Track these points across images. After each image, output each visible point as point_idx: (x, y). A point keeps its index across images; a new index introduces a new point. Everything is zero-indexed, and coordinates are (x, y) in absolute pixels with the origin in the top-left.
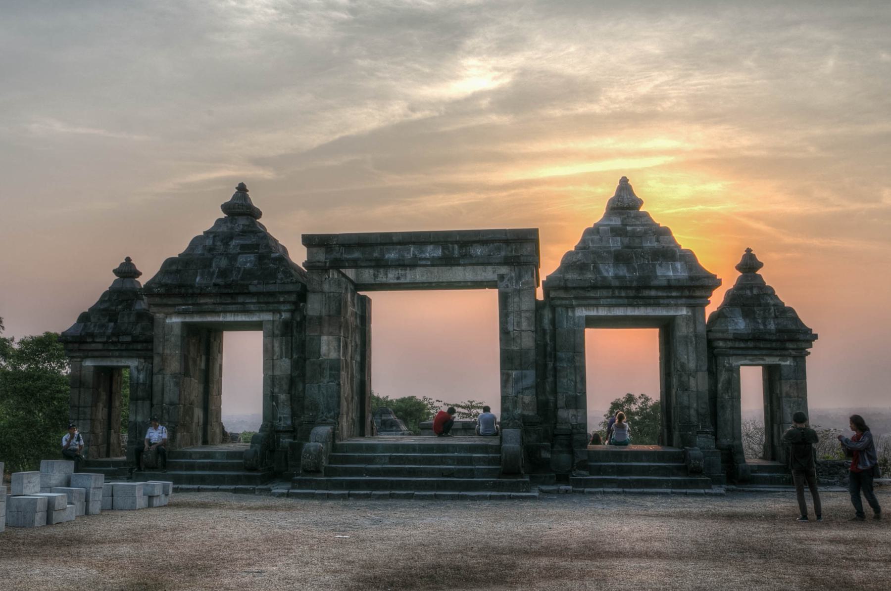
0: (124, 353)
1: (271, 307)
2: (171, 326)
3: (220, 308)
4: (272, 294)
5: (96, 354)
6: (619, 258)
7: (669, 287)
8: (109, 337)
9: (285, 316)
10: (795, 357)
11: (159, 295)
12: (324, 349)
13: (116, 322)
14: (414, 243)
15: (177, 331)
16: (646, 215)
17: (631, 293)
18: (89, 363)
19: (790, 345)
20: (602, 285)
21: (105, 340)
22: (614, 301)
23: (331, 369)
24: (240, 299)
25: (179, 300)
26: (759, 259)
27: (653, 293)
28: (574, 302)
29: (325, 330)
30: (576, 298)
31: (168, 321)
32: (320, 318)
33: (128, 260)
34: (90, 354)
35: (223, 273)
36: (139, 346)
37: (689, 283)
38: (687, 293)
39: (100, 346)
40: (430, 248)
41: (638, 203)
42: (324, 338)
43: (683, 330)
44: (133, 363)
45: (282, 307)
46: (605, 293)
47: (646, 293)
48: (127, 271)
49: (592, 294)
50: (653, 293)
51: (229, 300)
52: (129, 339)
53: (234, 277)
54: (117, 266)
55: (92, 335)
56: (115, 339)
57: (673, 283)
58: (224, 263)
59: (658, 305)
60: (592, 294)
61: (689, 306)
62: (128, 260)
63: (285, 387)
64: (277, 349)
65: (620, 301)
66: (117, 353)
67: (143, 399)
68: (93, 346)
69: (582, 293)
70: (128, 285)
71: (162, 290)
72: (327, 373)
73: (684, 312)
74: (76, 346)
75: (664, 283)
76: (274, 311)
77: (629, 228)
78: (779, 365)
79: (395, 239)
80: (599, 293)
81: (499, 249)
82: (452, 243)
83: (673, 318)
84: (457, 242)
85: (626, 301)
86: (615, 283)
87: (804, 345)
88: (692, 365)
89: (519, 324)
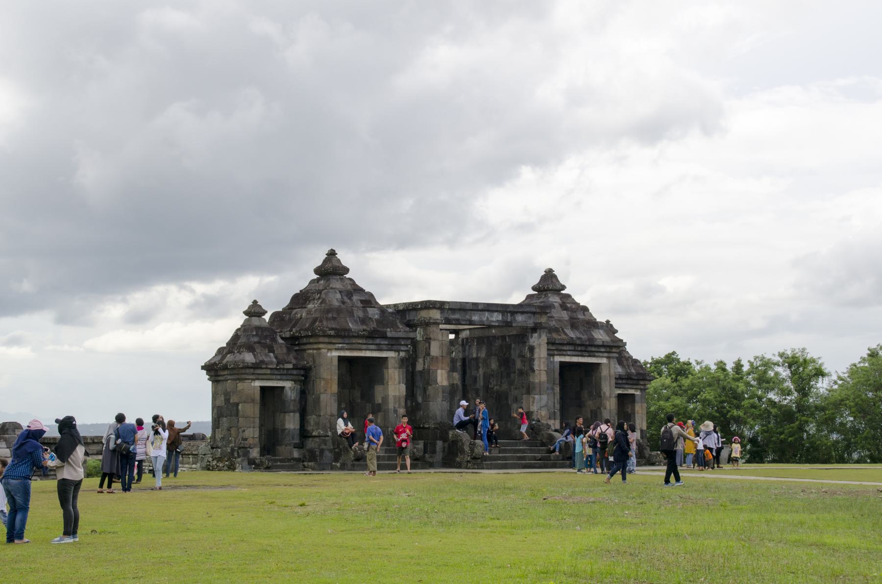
0: (284, 377)
1: (395, 347)
2: (332, 358)
3: (364, 347)
4: (398, 338)
5: (264, 377)
6: (574, 325)
7: (603, 346)
8: (277, 365)
9: (402, 354)
10: (641, 390)
11: (330, 336)
12: (439, 379)
13: (273, 352)
14: (488, 311)
15: (336, 362)
16: (568, 296)
17: (583, 348)
18: (258, 384)
19: (642, 383)
20: (571, 343)
21: (275, 366)
22: (574, 353)
23: (443, 392)
24: (378, 341)
25: (340, 340)
26: (615, 327)
27: (593, 349)
28: (556, 353)
29: (440, 365)
30: (557, 350)
31: (329, 354)
32: (437, 358)
33: (255, 302)
34: (260, 377)
35: (364, 321)
36: (295, 372)
37: (612, 344)
38: (608, 350)
39: (269, 372)
40: (496, 314)
41: (564, 287)
42: (439, 371)
43: (604, 372)
44: (288, 384)
45: (403, 348)
46: (571, 348)
47: (589, 349)
48: (254, 311)
49: (565, 348)
50: (593, 349)
51: (371, 342)
52: (291, 366)
53: (373, 325)
54: (246, 308)
55: (262, 362)
56: (281, 366)
57: (605, 344)
58: (361, 314)
59: (594, 356)
60: (565, 348)
61: (608, 358)
62: (255, 302)
63: (403, 404)
64: (397, 377)
65: (577, 353)
66: (279, 377)
67: (294, 412)
68: (264, 371)
69: (561, 347)
70: (255, 321)
71: (332, 333)
72: (440, 395)
73: (604, 361)
74: (252, 371)
75: (601, 343)
76: (398, 351)
77: (569, 305)
78: (633, 395)
79: (480, 307)
80: (567, 348)
81: (530, 318)
82: (507, 312)
83: (599, 364)
84: (510, 312)
85: (579, 353)
86: (578, 342)
87: (647, 382)
88: (608, 394)
89: (539, 366)
